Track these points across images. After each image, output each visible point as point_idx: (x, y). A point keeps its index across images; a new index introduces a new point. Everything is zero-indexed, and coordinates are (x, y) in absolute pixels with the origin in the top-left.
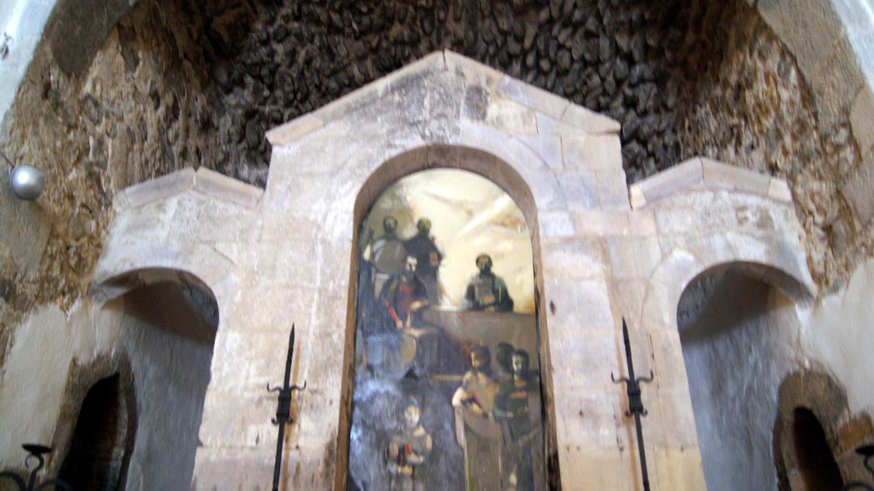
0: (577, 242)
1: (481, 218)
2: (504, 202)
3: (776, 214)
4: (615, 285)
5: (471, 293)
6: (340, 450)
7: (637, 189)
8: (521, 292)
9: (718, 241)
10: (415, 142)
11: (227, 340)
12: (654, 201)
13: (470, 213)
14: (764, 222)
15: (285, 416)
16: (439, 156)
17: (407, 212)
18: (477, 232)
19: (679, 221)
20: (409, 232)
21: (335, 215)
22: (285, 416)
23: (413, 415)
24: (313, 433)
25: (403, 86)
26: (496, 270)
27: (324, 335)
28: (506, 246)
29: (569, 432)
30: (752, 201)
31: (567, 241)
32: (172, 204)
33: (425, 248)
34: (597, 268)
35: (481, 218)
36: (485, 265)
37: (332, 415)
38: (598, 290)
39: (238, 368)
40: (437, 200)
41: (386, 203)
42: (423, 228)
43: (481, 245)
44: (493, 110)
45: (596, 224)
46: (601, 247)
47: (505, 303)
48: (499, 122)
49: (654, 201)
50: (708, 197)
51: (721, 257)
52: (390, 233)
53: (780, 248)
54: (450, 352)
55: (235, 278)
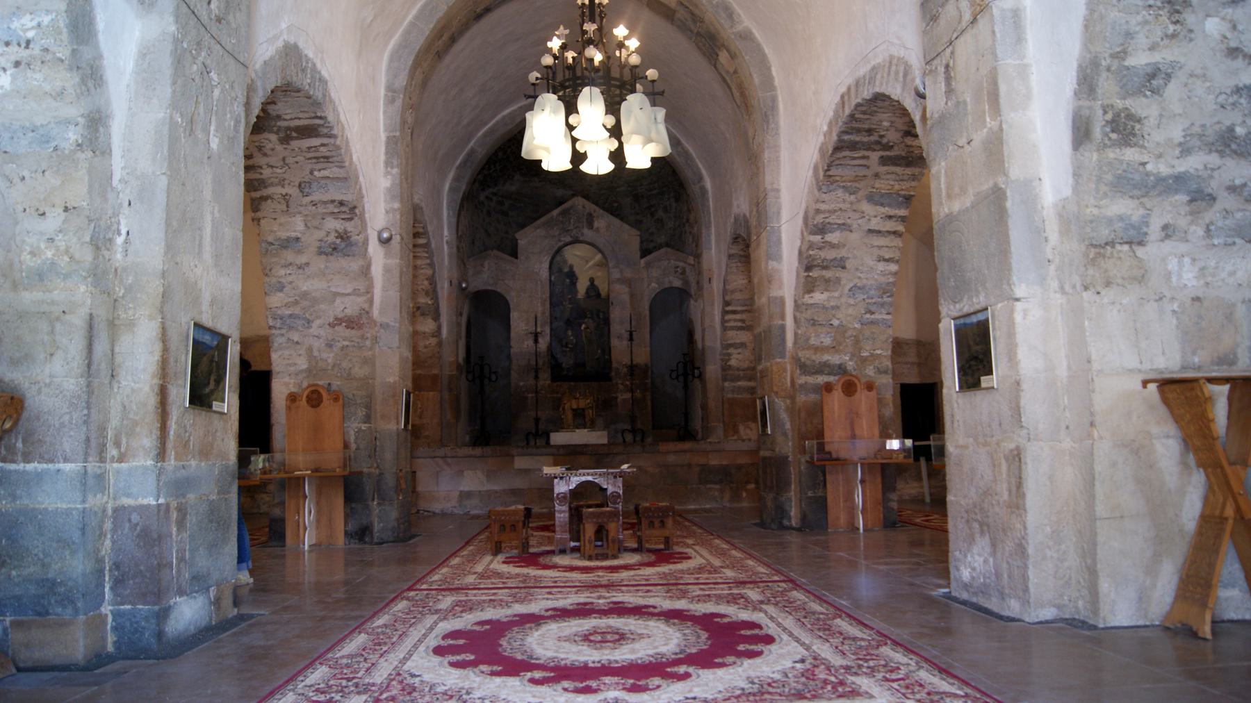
0: (623, 281)
1: (591, 264)
2: (599, 256)
3: (688, 270)
4: (632, 296)
5: (587, 292)
6: (550, 348)
7: (643, 261)
8: (603, 293)
9: (666, 280)
10: (568, 239)
11: (514, 315)
12: (648, 265)
13: (587, 262)
14: (684, 272)
15: (536, 341)
16: (576, 241)
17: (565, 262)
18: (590, 268)
19: (655, 273)
20: (566, 270)
21: (542, 268)
22: (536, 341)
23: (570, 333)
24: (544, 343)
25: (564, 213)
26: (596, 283)
27: (543, 313)
28: (599, 274)
29: (615, 342)
30: (681, 264)
31: (618, 280)
32: (486, 264)
33: (572, 276)
34: (627, 290)
35: (591, 264)
36: (592, 280)
37: (548, 338)
38: (626, 298)
39: (519, 324)
40: (577, 256)
41: (558, 258)
42: (571, 267)
43: (591, 273)
44: (596, 224)
45: (628, 274)
46: (628, 282)
47: (598, 295)
48: (598, 230)
49: (648, 265)
50: (666, 263)
51: (667, 286)
52: (560, 271)
53: (686, 282)
54: (581, 312)
55: (513, 294)
